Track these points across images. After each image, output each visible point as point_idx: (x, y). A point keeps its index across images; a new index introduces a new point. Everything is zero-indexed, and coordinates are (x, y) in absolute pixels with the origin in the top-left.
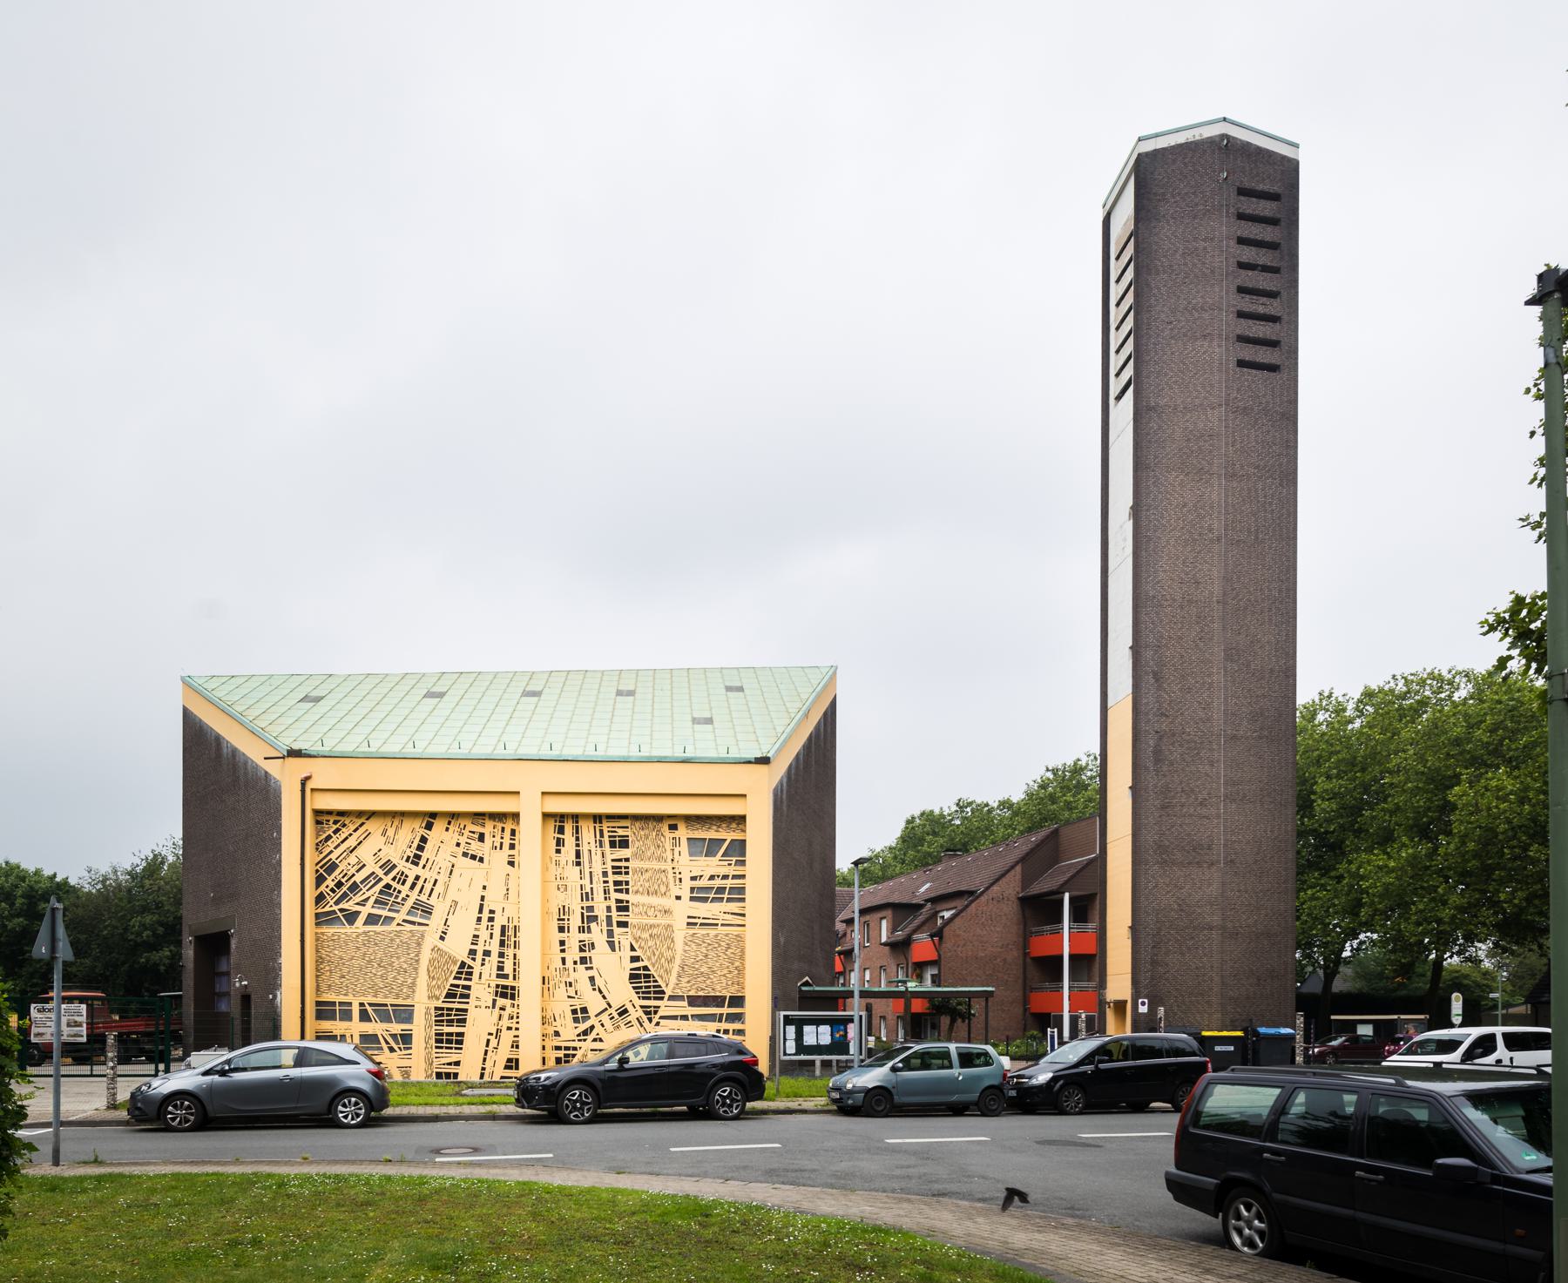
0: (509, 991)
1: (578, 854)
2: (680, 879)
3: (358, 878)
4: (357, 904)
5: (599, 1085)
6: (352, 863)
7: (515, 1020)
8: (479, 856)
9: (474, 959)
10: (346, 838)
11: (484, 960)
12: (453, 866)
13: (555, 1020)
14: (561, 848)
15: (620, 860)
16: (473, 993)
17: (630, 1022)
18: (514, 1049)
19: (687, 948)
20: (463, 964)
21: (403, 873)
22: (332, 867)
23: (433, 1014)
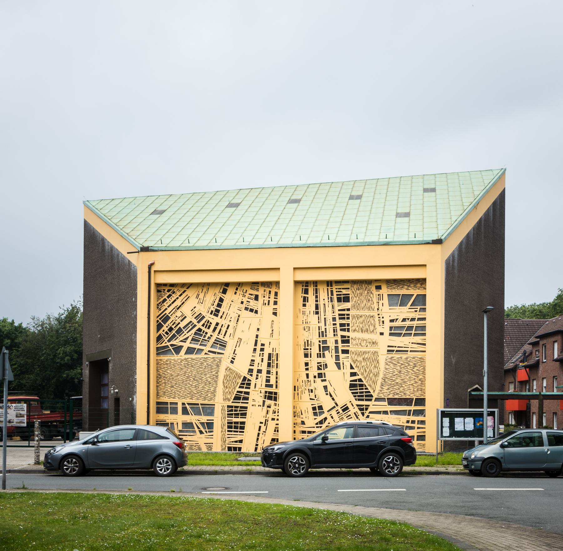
0: (273, 395)
1: (317, 307)
2: (383, 322)
3: (182, 325)
4: (181, 341)
5: (309, 453)
6: (179, 316)
7: (276, 414)
8: (255, 309)
9: (251, 375)
10: (175, 301)
11: (257, 375)
12: (239, 316)
13: (302, 414)
14: (306, 303)
15: (344, 310)
16: (251, 397)
17: (350, 415)
18: (276, 433)
19: (387, 367)
20: (245, 378)
21: (209, 321)
22: (166, 319)
23: (226, 410)
